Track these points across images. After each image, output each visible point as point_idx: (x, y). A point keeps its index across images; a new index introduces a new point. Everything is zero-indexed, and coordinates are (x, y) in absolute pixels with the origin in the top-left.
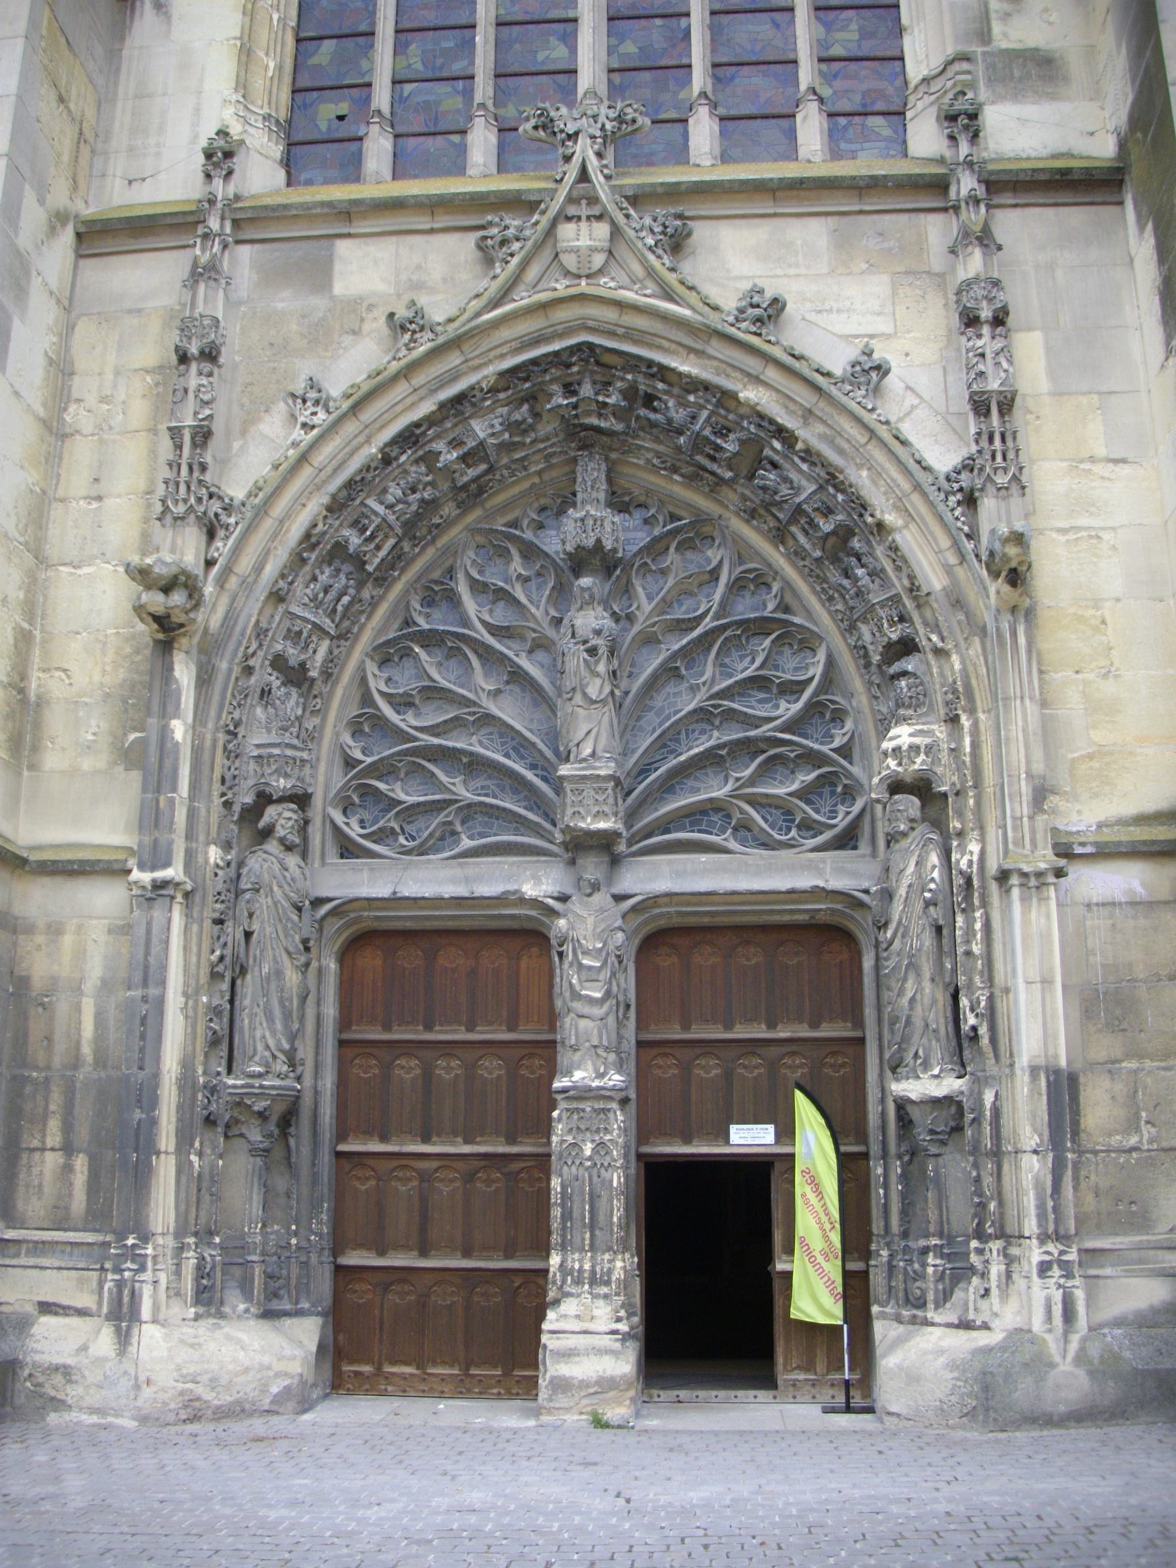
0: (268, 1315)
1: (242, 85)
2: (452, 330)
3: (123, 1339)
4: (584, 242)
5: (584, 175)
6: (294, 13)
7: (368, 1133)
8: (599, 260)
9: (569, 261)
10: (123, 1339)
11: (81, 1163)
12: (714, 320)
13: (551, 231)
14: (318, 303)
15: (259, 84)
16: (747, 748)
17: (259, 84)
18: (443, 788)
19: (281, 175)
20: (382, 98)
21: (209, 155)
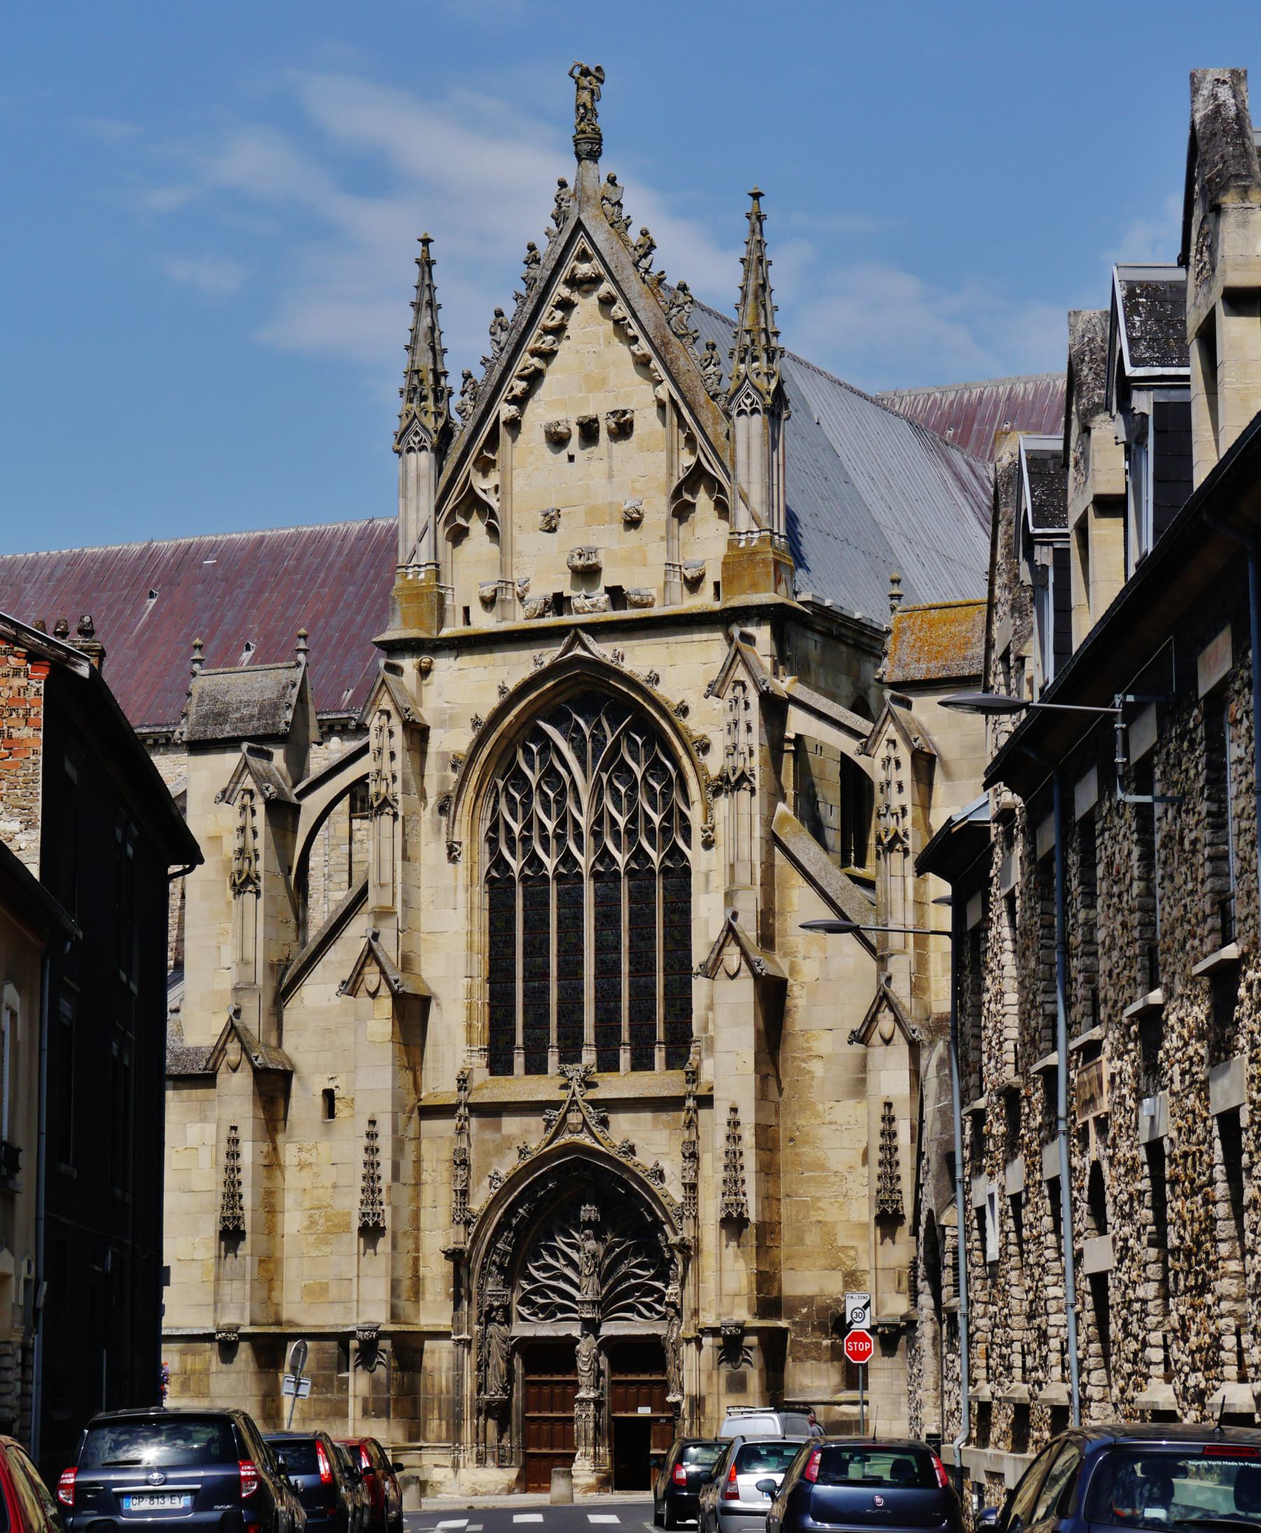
0: (500, 1467)
1: (470, 1042)
2: (535, 1154)
3: (456, 1473)
4: (574, 1121)
5: (574, 1095)
6: (487, 995)
7: (534, 1410)
8: (580, 1127)
9: (571, 1127)
10: (456, 1473)
11: (444, 1423)
12: (613, 1152)
13: (564, 1118)
14: (497, 1136)
15: (475, 1036)
16: (636, 1288)
17: (475, 1036)
18: (549, 1298)
19: (487, 1071)
20: (519, 1040)
21: (459, 1081)
